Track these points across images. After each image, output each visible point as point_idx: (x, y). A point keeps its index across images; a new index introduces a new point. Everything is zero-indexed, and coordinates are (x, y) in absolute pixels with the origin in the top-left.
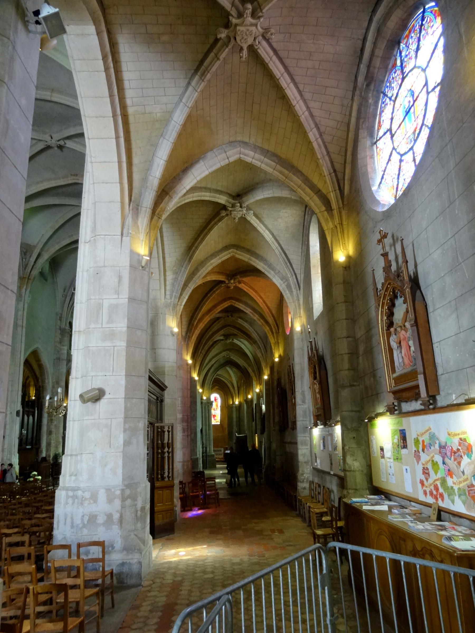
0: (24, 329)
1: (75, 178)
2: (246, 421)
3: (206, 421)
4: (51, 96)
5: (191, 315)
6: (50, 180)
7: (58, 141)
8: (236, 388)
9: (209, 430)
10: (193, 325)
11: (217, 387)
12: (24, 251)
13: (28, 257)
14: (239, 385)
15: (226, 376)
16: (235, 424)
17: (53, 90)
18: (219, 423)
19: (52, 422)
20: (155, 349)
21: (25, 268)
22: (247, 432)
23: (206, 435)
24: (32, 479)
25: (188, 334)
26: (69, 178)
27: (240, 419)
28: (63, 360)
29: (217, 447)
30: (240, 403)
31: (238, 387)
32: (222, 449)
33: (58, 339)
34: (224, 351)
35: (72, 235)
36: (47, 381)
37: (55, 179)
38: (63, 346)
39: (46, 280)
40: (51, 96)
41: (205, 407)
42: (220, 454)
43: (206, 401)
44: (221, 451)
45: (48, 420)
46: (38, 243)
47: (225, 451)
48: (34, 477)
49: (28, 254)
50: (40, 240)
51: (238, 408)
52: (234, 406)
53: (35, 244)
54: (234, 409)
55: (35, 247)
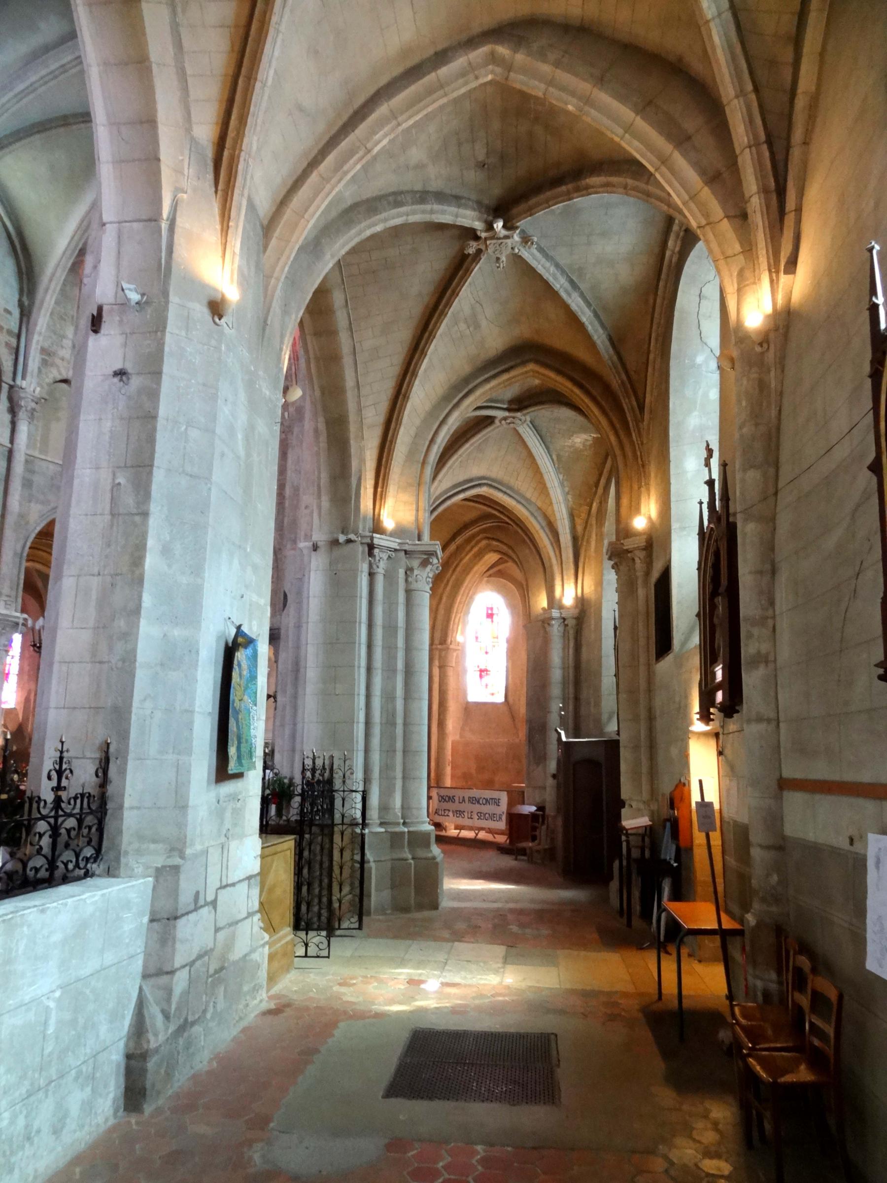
2: (608, 680)
3: (390, 649)
8: (566, 538)
9: (408, 696)
11: (492, 558)
14: (579, 529)
15: (524, 484)
16: (556, 690)
18: (500, 698)
22: (612, 727)
23: (389, 722)
27: (580, 676)
29: (489, 785)
30: (582, 603)
31: (575, 539)
32: (504, 797)
34: (471, 43)
41: (390, 577)
42: (492, 817)
43: (394, 543)
44: (497, 802)
47: (511, 804)
51: (571, 623)
52: (555, 613)
54: (556, 629)
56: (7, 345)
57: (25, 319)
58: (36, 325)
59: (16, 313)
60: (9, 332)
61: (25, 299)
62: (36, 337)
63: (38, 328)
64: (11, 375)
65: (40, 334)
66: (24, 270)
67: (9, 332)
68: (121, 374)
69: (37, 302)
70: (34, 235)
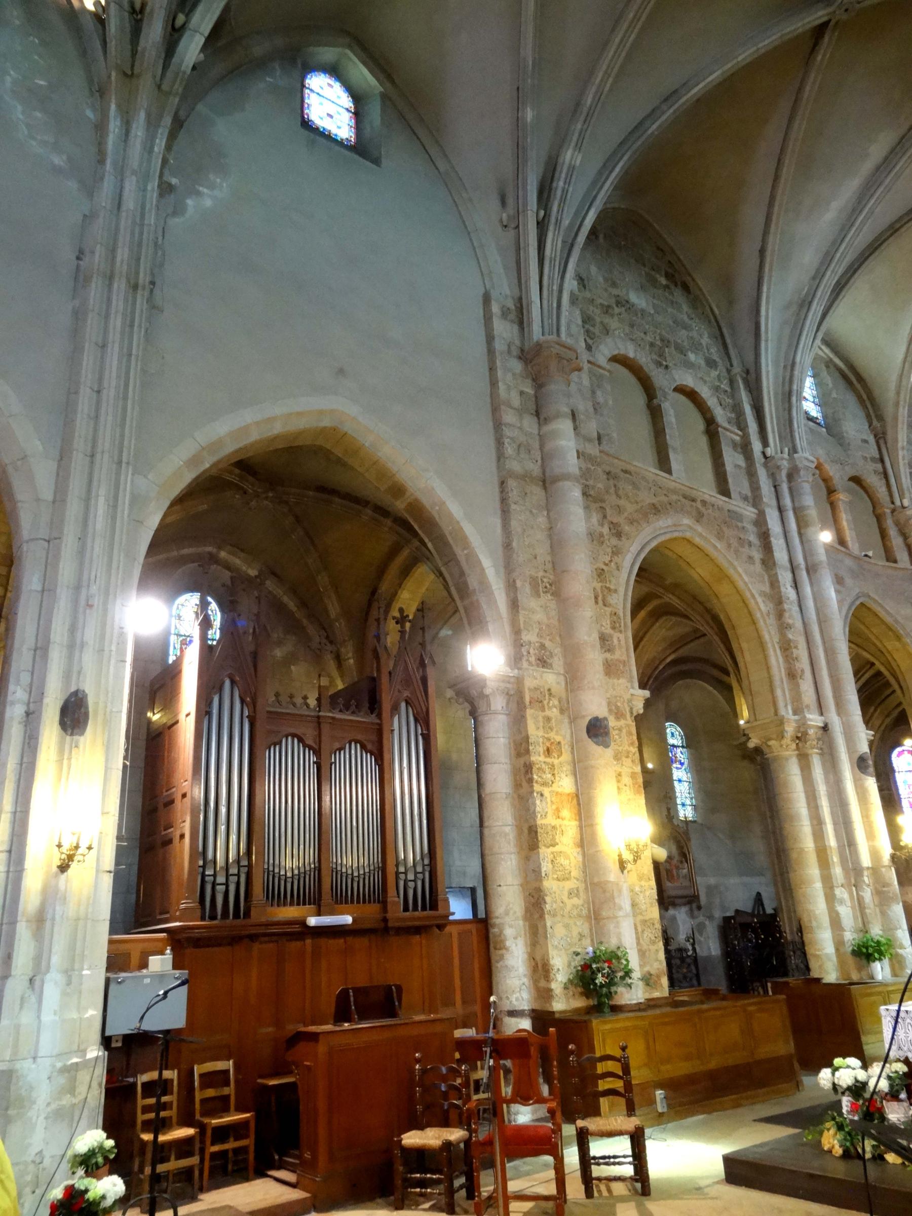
19: (530, 781)
39: (377, 161)
45: (515, 772)
56: (875, 472)
57: (881, 442)
58: (896, 440)
59: (871, 439)
60: (873, 459)
61: (875, 422)
62: (901, 453)
63: (900, 445)
64: (888, 499)
65: (903, 448)
66: (865, 397)
67: (873, 459)
69: (889, 419)
70: (866, 362)
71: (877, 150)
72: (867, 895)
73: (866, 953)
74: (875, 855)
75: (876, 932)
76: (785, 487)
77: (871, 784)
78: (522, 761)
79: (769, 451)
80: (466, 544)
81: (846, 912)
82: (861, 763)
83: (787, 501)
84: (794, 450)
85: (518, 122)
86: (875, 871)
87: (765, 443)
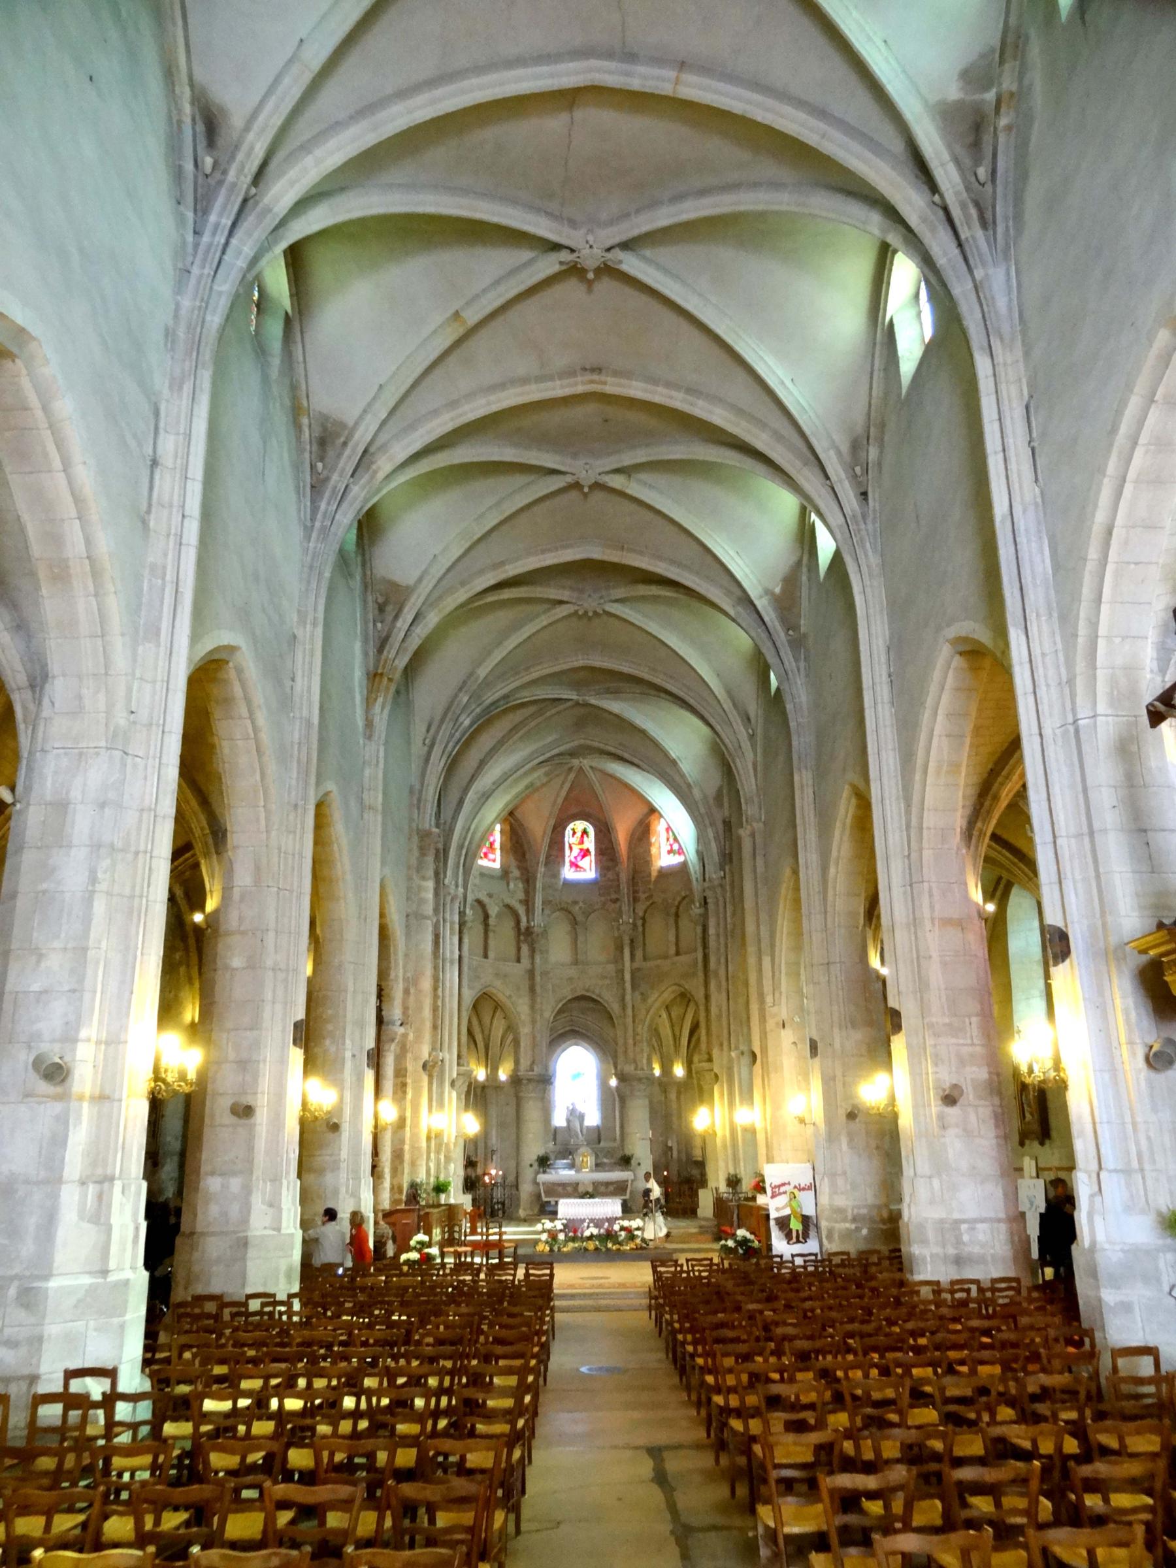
0: (379, 818)
1: (595, 377)
4: (677, 82)
5: (990, 766)
6: (524, 381)
7: (608, 250)
10: (996, 798)
12: (380, 600)
13: (389, 618)
17: (682, 65)
20: (1145, 831)
21: (380, 650)
24: (414, 1256)
25: (979, 824)
26: (579, 379)
28: (426, 918)
33: (414, 861)
35: (502, 563)
36: (392, 975)
37: (539, 379)
38: (424, 878)
40: (677, 82)
45: (395, 1085)
46: (420, 580)
48: (419, 1251)
49: (389, 608)
50: (425, 572)
53: (411, 582)
55: (408, 591)
68: (794, 1043)
71: (550, 739)
72: (442, 1157)
73: (440, 1189)
74: (449, 1138)
75: (442, 1178)
76: (448, 906)
77: (454, 1094)
78: (400, 1079)
79: (447, 882)
80: (396, 954)
81: (432, 1165)
82: (453, 1084)
83: (448, 916)
84: (457, 886)
85: (456, 696)
86: (447, 1145)
87: (445, 876)
